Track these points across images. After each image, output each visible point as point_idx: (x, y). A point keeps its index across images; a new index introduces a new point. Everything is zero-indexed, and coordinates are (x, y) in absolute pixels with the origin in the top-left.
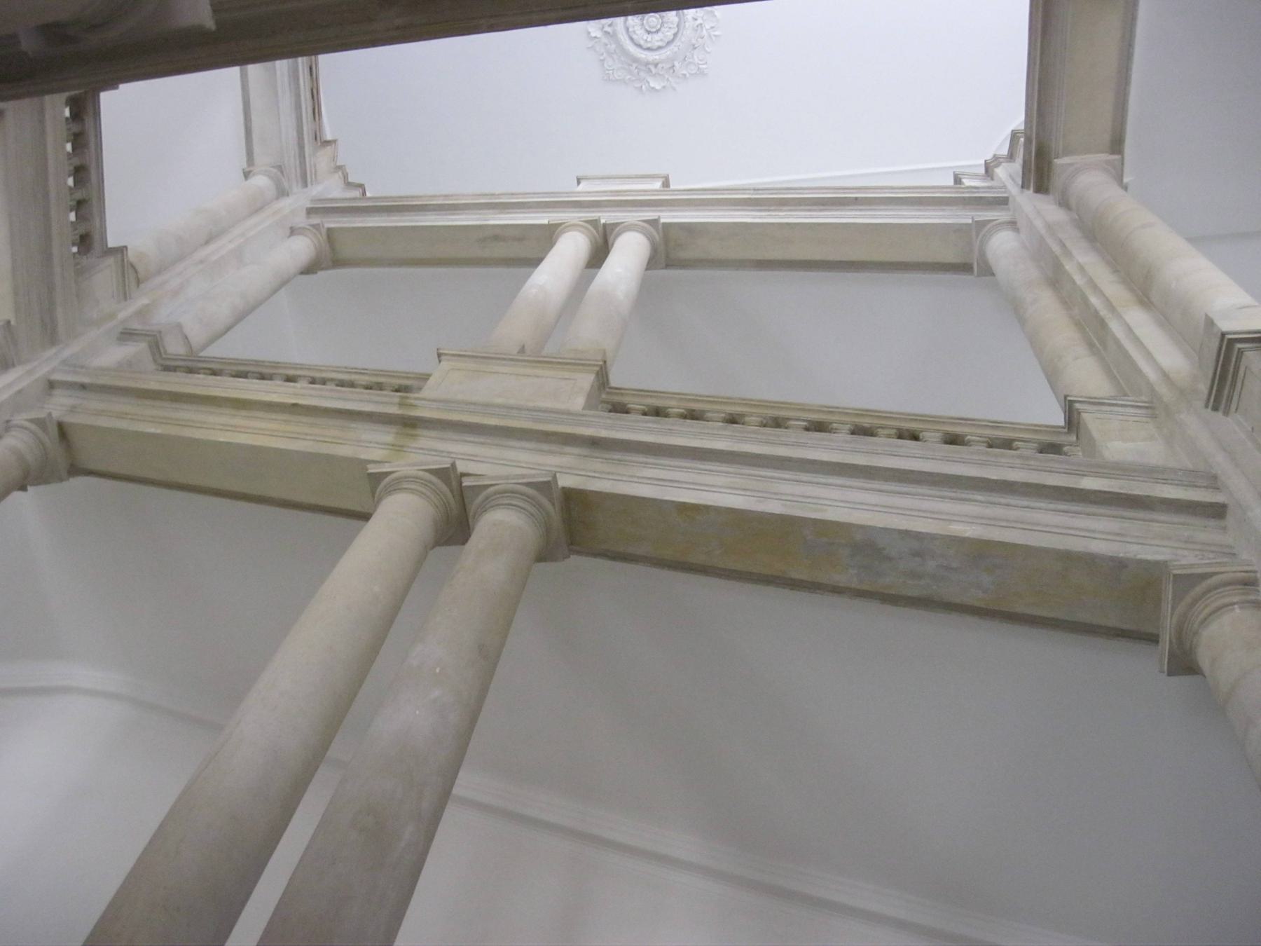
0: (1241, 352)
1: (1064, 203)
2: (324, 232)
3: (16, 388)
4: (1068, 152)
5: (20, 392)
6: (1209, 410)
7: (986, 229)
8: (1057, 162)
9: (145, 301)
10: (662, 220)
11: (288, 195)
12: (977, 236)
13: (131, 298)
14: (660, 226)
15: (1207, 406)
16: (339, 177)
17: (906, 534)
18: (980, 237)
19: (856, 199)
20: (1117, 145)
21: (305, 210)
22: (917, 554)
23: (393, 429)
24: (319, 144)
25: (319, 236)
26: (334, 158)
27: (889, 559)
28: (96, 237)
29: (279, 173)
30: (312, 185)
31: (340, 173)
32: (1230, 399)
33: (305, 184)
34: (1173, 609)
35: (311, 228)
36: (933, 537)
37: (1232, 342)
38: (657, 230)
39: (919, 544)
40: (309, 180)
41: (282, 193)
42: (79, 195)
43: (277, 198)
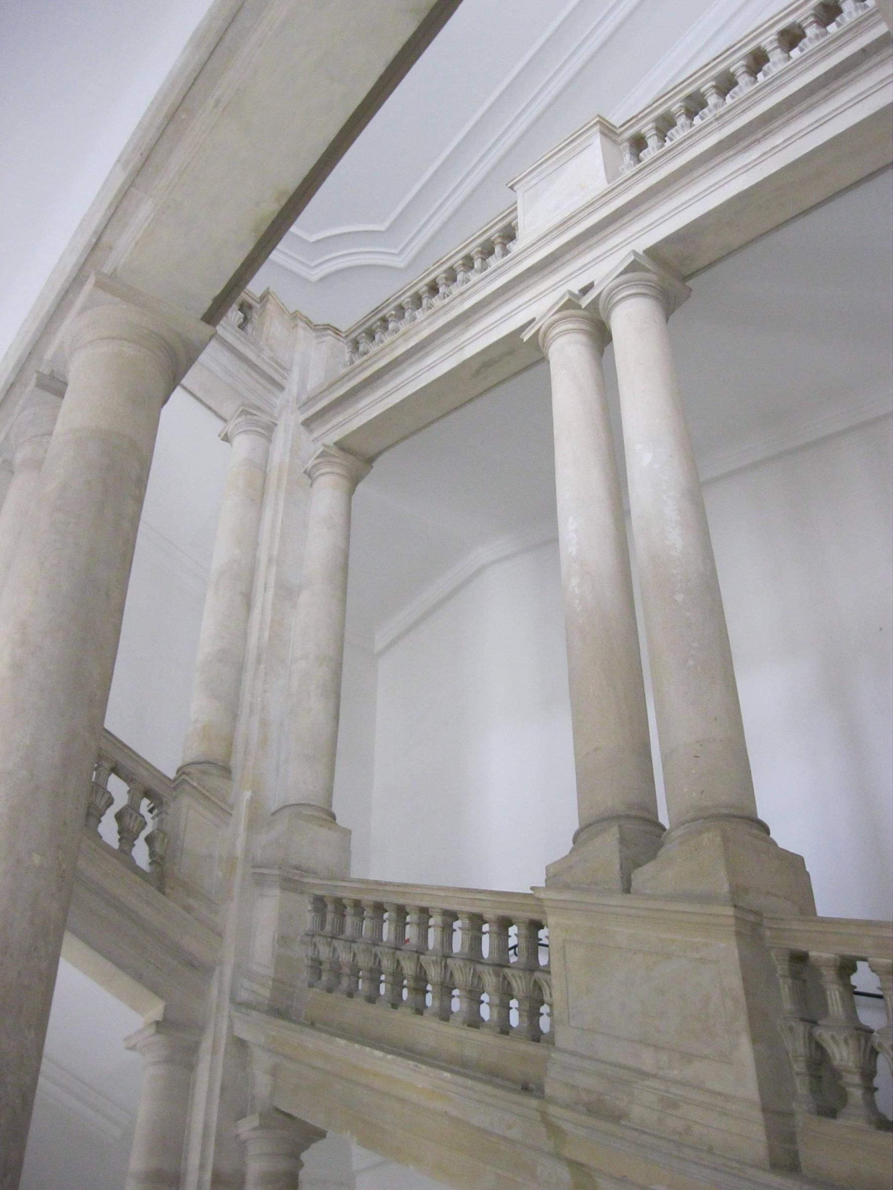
2: (334, 451)
3: (217, 1091)
5: (223, 1089)
9: (248, 794)
10: (640, 251)
11: (276, 425)
13: (232, 807)
14: (647, 263)
16: (304, 329)
21: (302, 428)
24: (259, 306)
25: (337, 460)
26: (282, 310)
28: (155, 785)
29: (249, 417)
30: (286, 379)
31: (300, 323)
33: (281, 388)
35: (320, 460)
38: (648, 271)
40: (277, 378)
41: (270, 429)
42: (107, 765)
43: (269, 440)
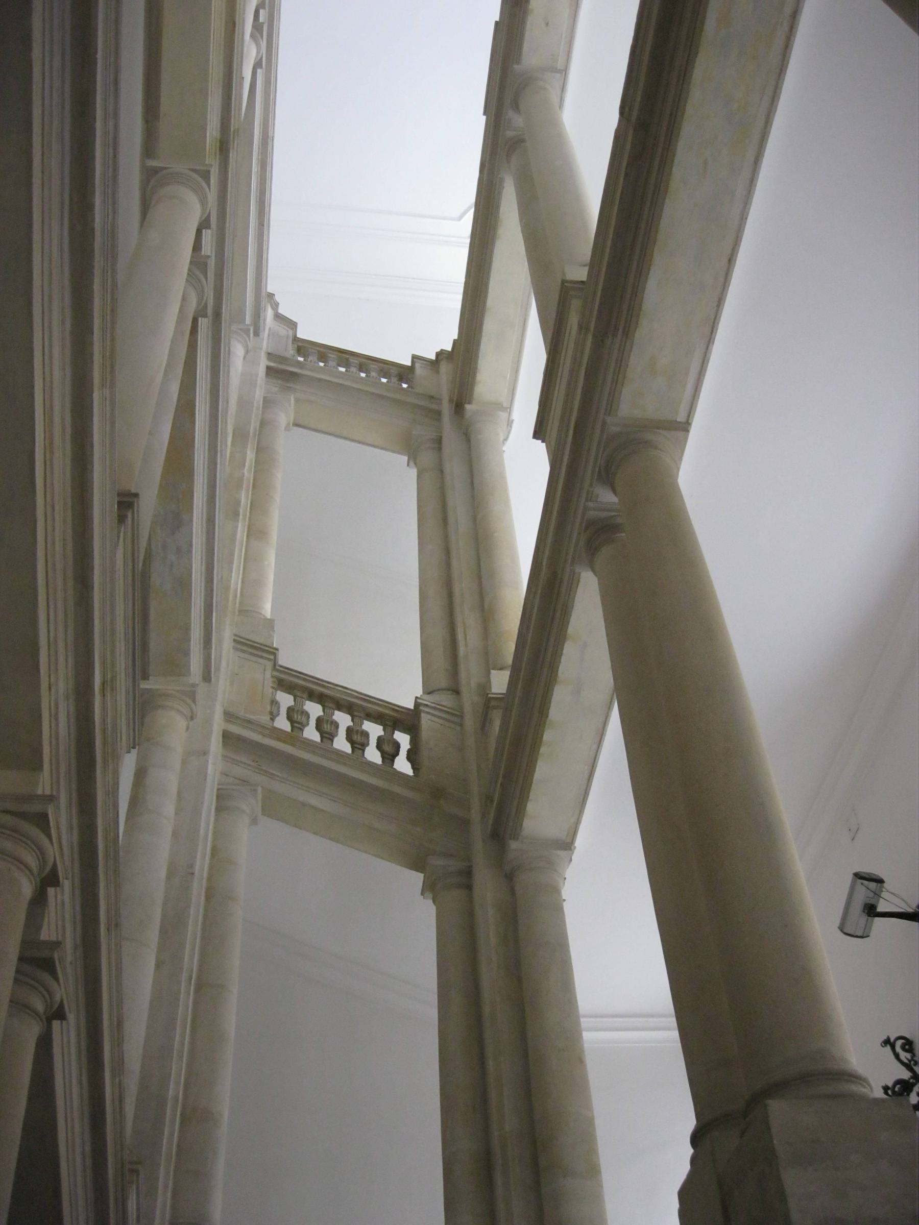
0: (269, 659)
1: (268, 402)
4: (297, 401)
6: (234, 637)
7: (245, 336)
8: (293, 395)
12: (241, 329)
15: (235, 635)
17: (191, 546)
18: (239, 331)
19: (263, 225)
20: (297, 425)
22: (179, 551)
23: (218, 137)
27: (173, 534)
32: (244, 651)
34: (178, 691)
36: (190, 559)
37: (275, 654)
39: (185, 551)
